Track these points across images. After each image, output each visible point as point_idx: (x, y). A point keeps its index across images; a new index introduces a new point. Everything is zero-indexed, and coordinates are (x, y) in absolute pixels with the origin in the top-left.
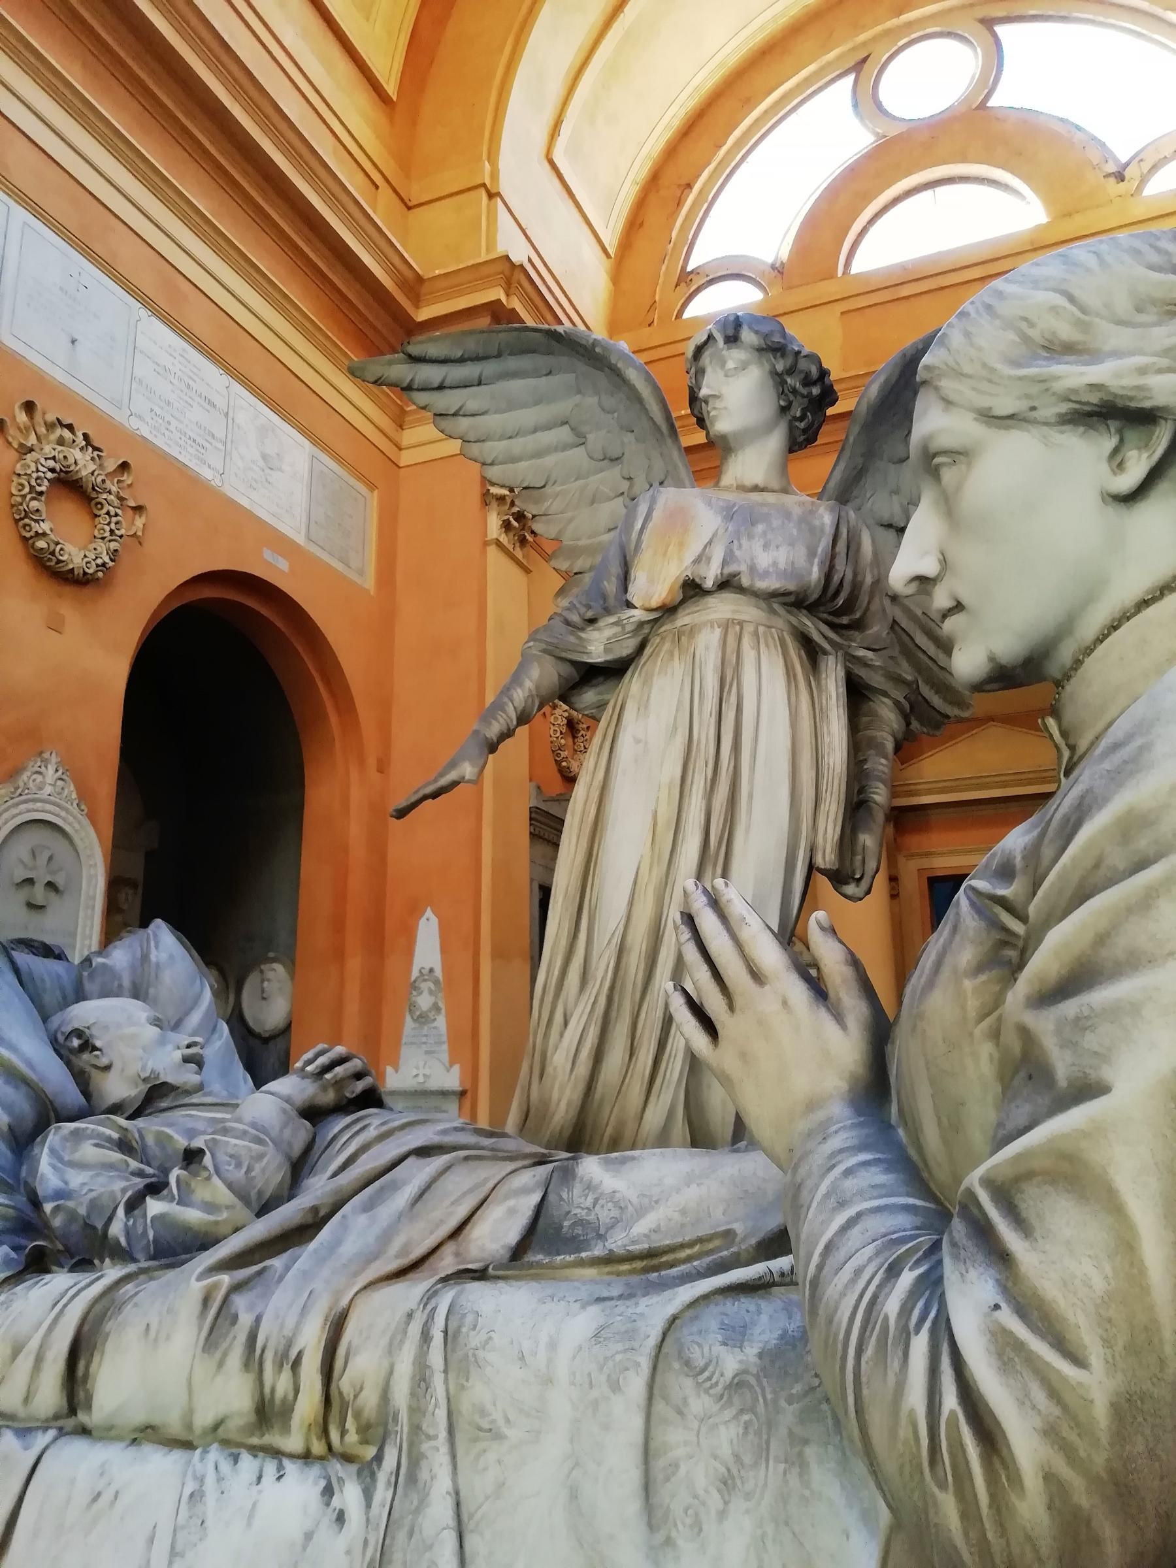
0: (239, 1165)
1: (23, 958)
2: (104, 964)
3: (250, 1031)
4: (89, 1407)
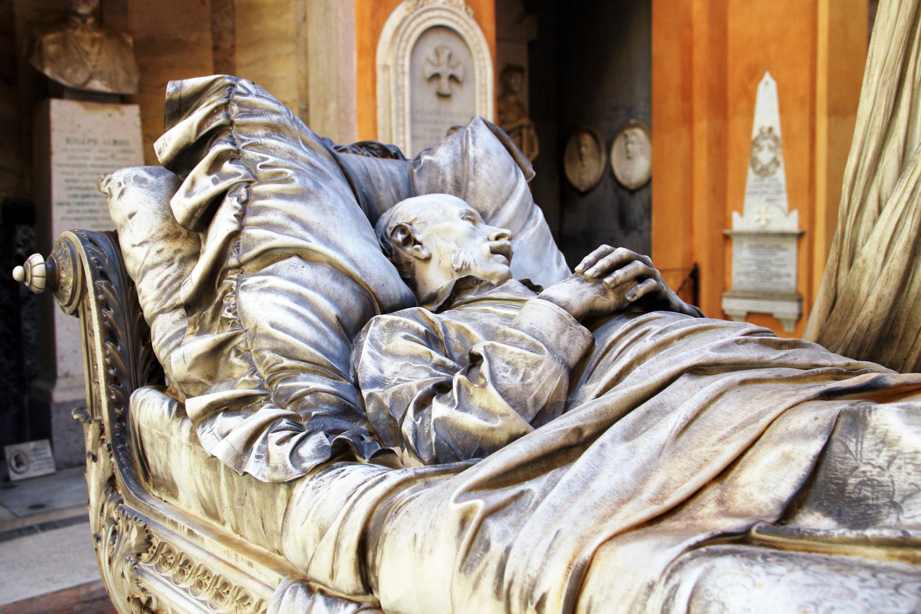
0: (515, 372)
1: (357, 162)
2: (430, 162)
3: (619, 185)
4: (378, 591)
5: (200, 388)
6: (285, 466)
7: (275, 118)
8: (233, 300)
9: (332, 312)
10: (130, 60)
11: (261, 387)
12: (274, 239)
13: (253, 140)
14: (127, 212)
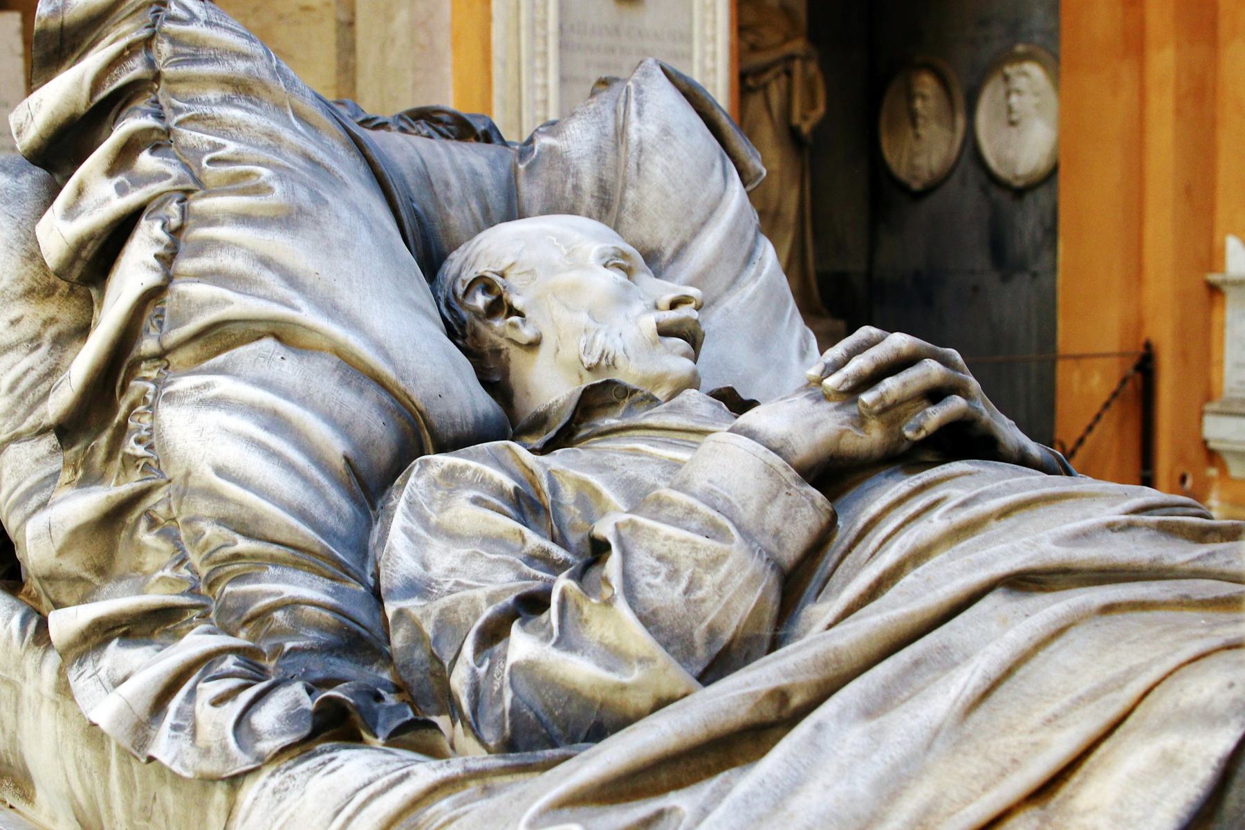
0: (673, 576)
2: (552, 149)
5: (80, 590)
6: (224, 747)
7: (241, 66)
8: (146, 421)
9: (336, 447)
11: (193, 592)
12: (228, 302)
13: (198, 110)
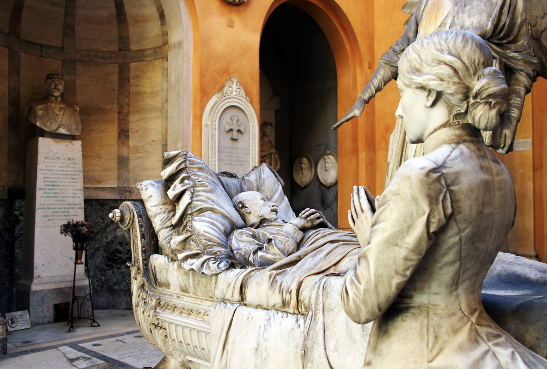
0: (282, 243)
1: (224, 179)
2: (248, 179)
3: (322, 184)
4: (246, 300)
7: (200, 165)
8: (190, 224)
10: (78, 118)
13: (194, 173)
14: (149, 195)
